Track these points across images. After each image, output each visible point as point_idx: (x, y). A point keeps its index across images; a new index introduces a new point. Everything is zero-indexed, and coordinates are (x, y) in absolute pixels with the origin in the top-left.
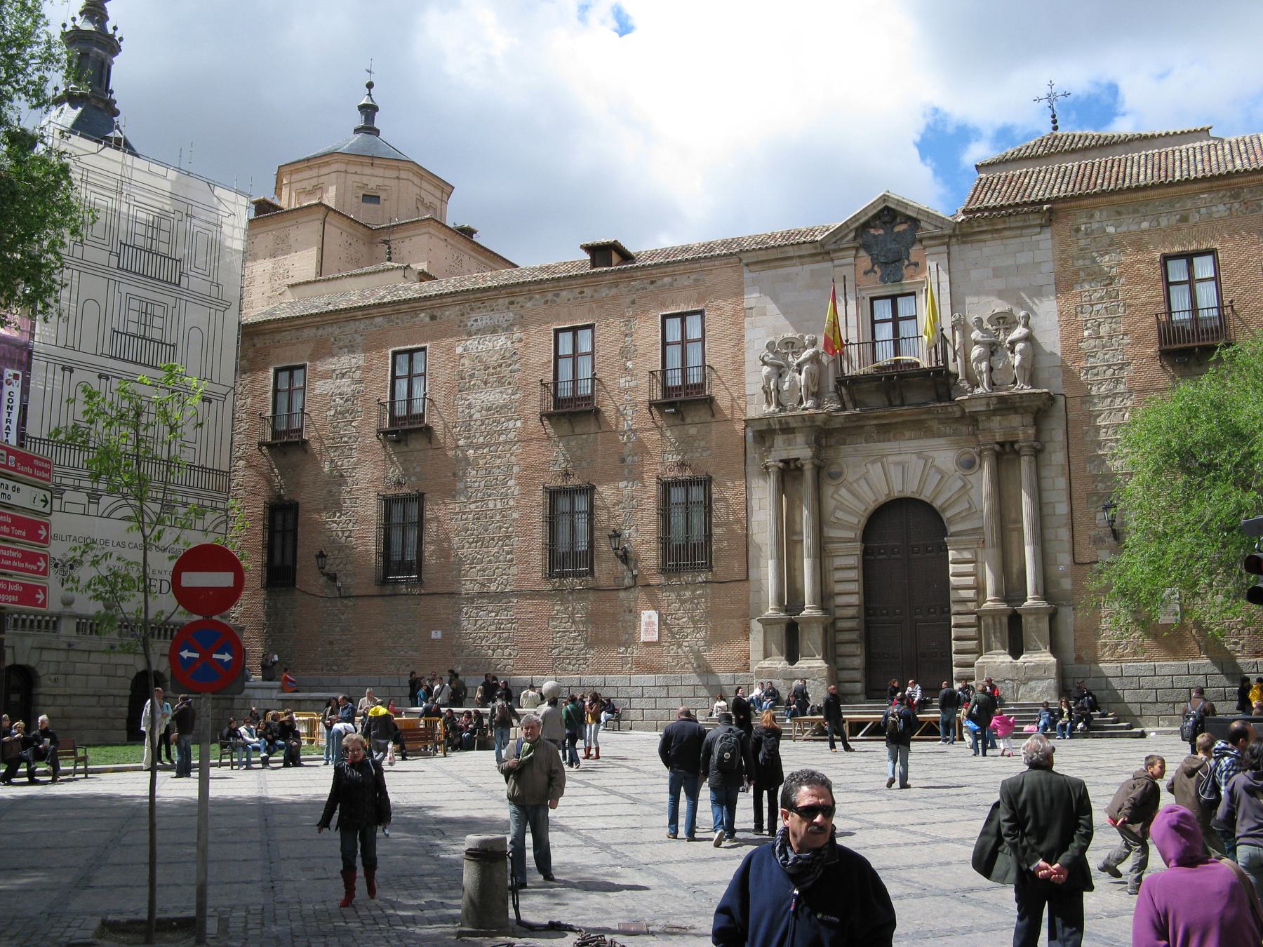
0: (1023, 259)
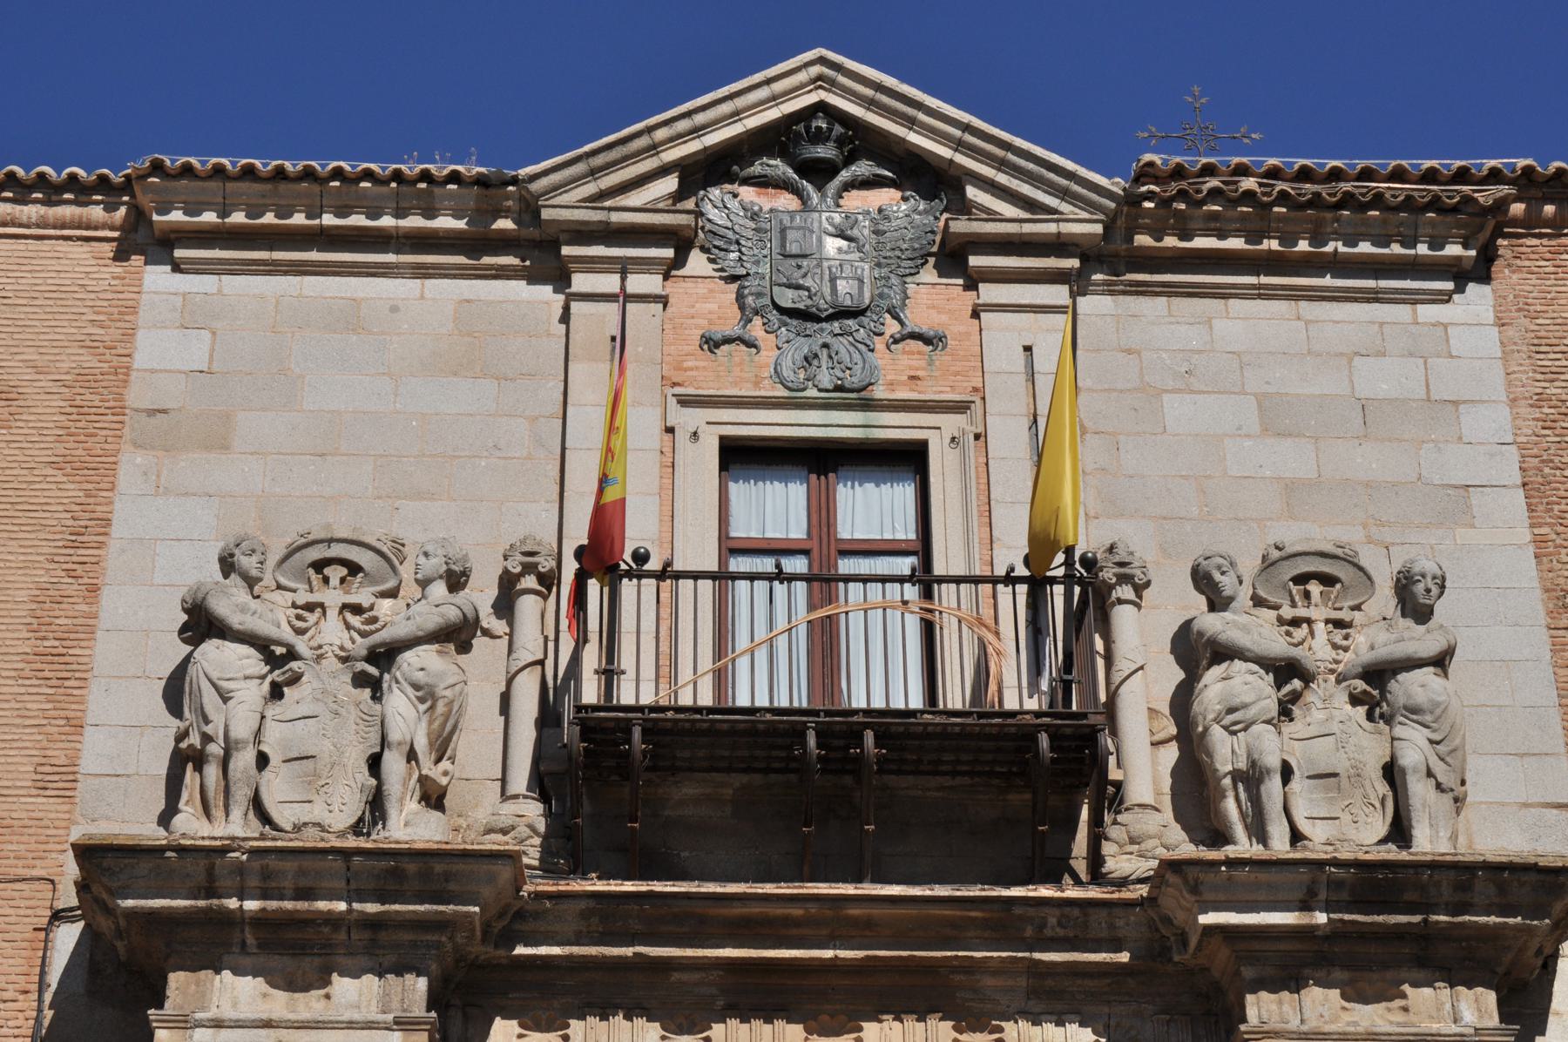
0: (1383, 379)
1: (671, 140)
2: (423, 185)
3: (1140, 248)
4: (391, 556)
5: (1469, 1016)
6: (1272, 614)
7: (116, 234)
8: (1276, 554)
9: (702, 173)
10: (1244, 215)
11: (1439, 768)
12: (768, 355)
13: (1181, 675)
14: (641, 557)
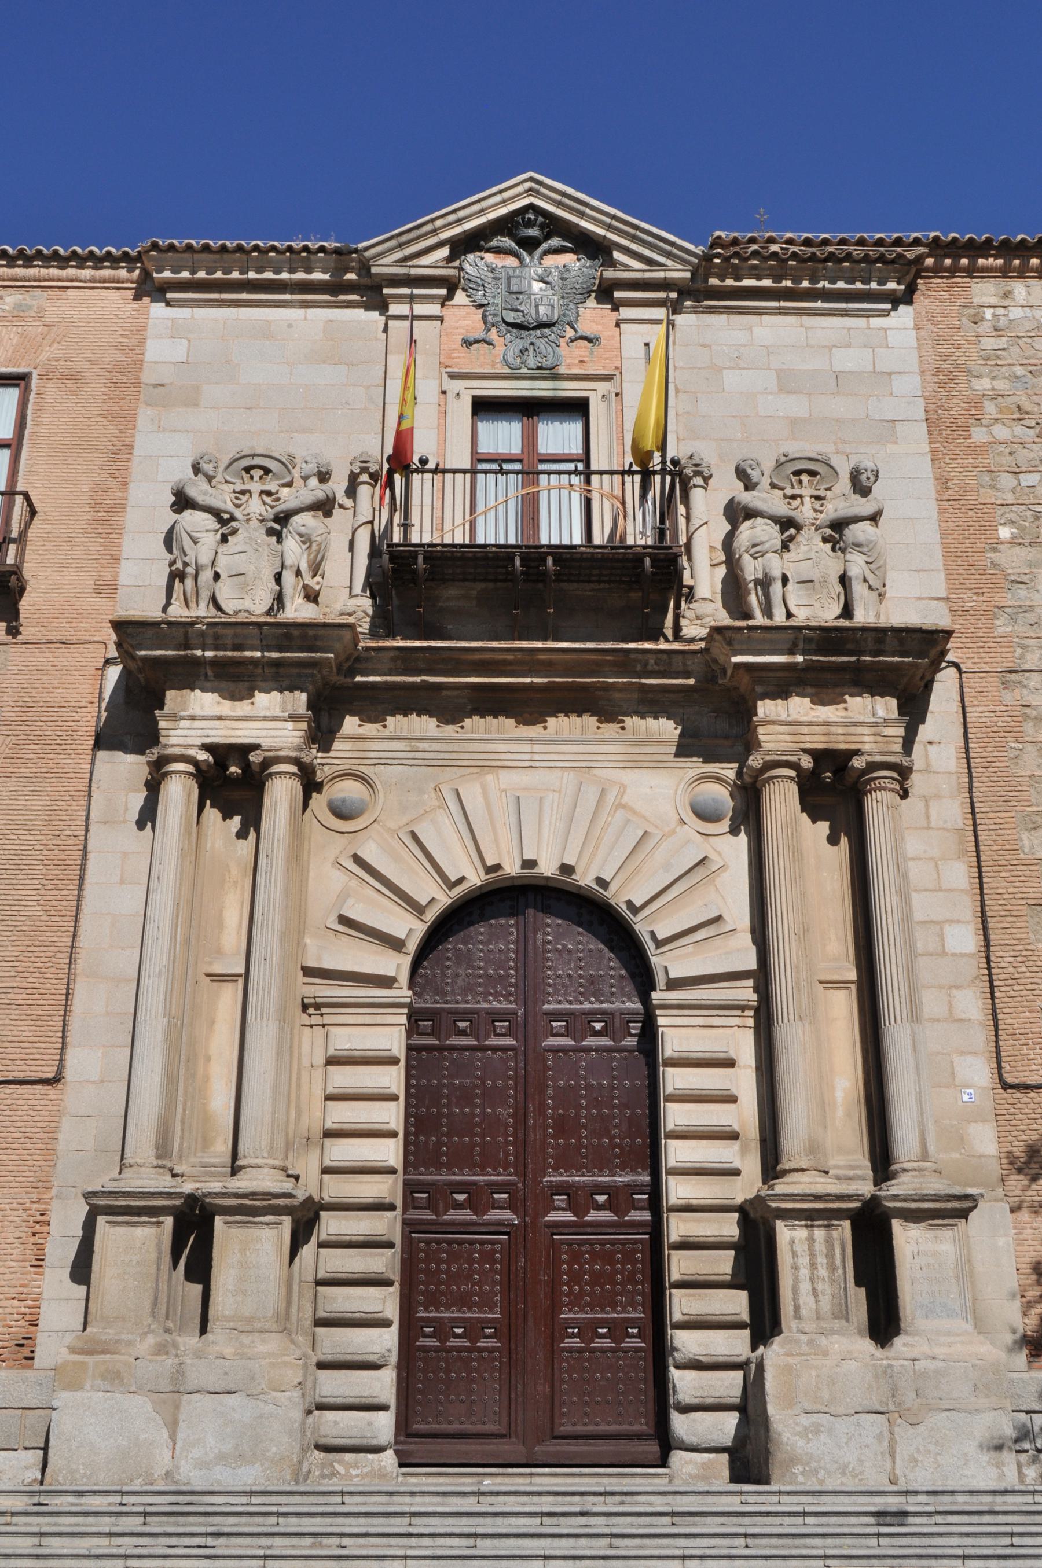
0: (848, 360)
1: (445, 226)
2: (304, 254)
3: (712, 286)
4: (287, 464)
5: (881, 713)
6: (780, 493)
7: (134, 285)
8: (783, 459)
9: (465, 245)
10: (772, 267)
11: (870, 577)
12: (500, 349)
13: (729, 527)
14: (423, 461)
